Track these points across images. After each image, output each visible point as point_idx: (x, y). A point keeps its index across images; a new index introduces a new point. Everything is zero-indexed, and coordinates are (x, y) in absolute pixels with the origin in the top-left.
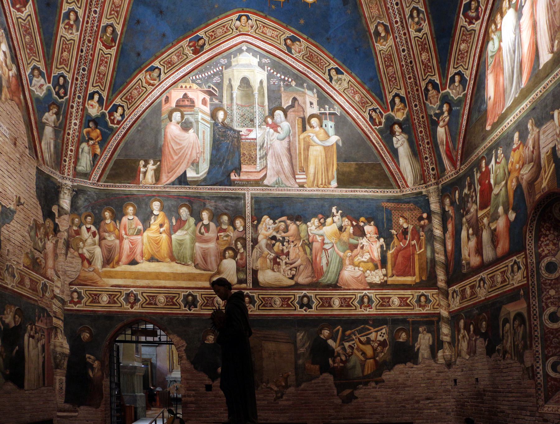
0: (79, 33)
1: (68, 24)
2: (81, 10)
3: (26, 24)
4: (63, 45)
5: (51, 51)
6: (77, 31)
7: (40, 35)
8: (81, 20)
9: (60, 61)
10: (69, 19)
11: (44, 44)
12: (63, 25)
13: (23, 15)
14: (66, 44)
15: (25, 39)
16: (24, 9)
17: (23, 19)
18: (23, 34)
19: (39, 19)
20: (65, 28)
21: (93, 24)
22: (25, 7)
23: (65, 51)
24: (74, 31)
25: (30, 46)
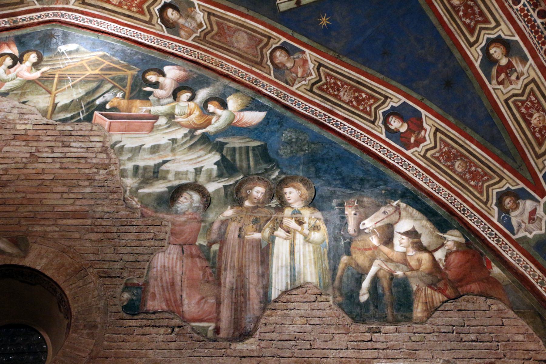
0: (531, 61)
1: (501, 70)
2: (503, 26)
3: (441, 150)
4: (519, 111)
5: (508, 142)
6: (524, 60)
7: (471, 140)
8: (517, 38)
9: (536, 139)
10: (496, 62)
11: (489, 145)
12: (494, 82)
13: (428, 142)
14: (523, 102)
15: (454, 171)
16: (423, 133)
17: (431, 149)
18: (448, 167)
19: (451, 119)
20: (499, 83)
21: (529, 21)
22: (421, 128)
23: (531, 115)
24: (520, 68)
25: (470, 172)
